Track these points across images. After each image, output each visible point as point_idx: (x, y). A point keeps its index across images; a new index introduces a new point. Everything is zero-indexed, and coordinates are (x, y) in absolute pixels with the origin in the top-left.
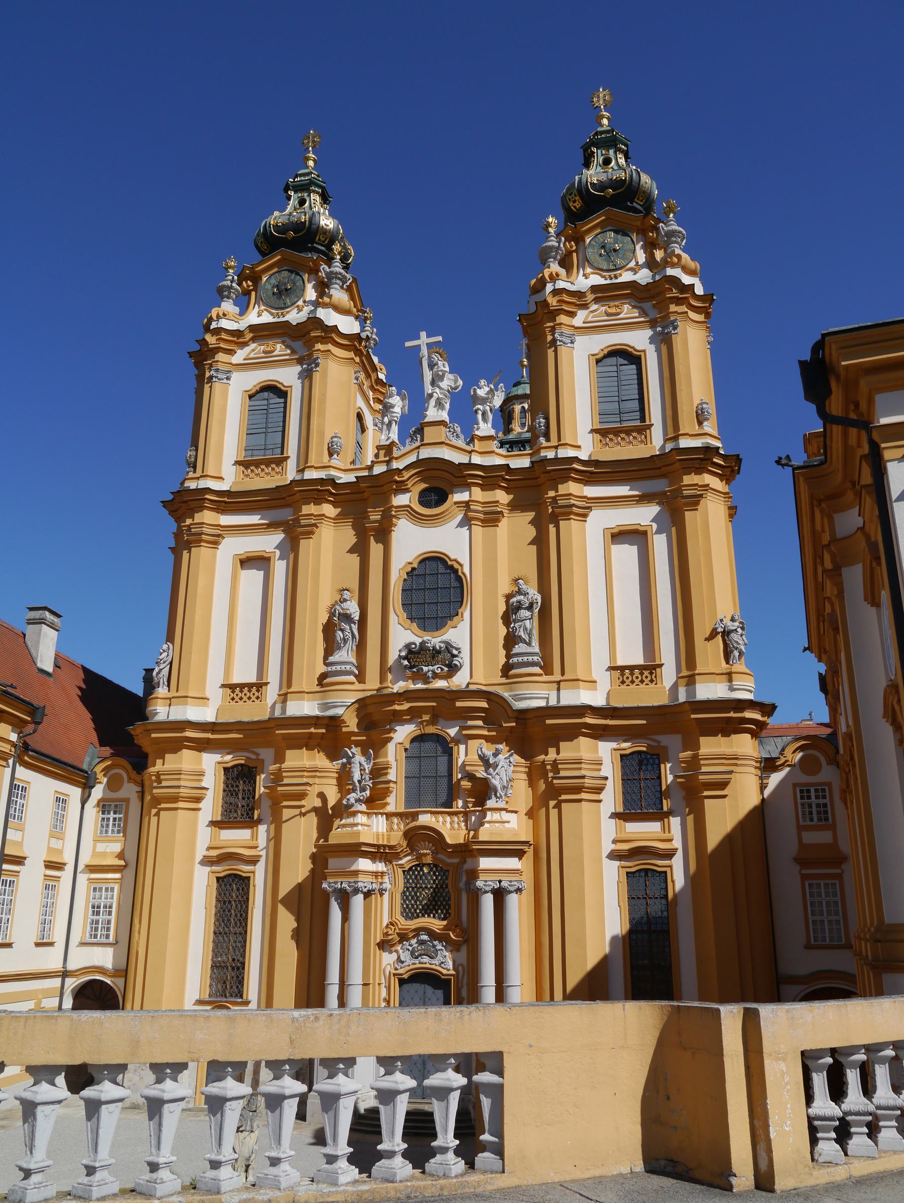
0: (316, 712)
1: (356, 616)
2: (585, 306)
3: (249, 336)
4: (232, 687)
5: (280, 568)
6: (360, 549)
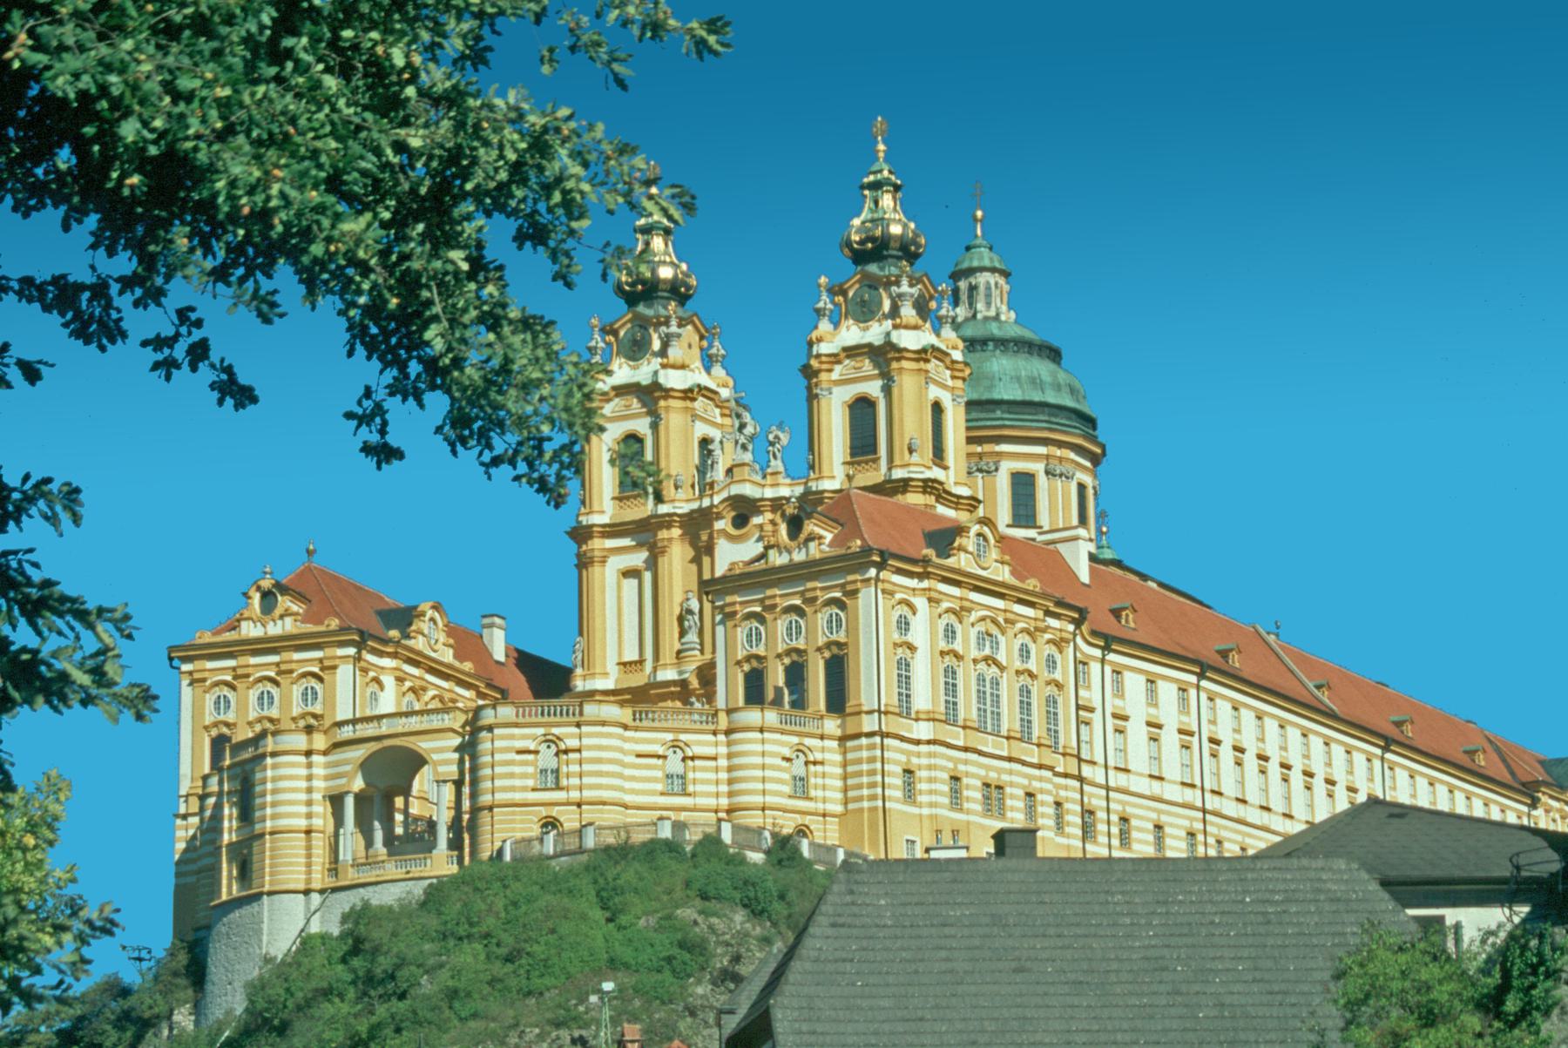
0: (676, 677)
1: (696, 610)
2: (839, 362)
3: (613, 394)
4: (624, 664)
5: (647, 576)
6: (697, 560)
